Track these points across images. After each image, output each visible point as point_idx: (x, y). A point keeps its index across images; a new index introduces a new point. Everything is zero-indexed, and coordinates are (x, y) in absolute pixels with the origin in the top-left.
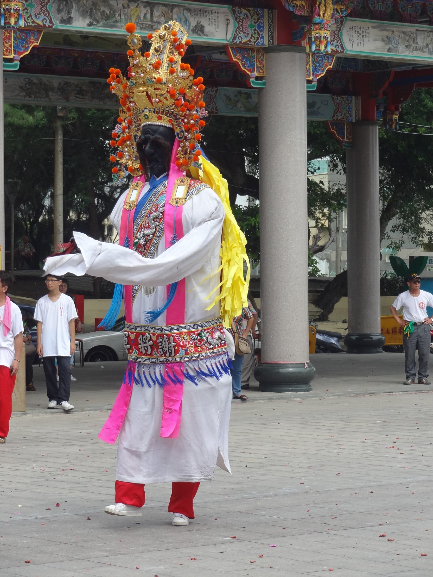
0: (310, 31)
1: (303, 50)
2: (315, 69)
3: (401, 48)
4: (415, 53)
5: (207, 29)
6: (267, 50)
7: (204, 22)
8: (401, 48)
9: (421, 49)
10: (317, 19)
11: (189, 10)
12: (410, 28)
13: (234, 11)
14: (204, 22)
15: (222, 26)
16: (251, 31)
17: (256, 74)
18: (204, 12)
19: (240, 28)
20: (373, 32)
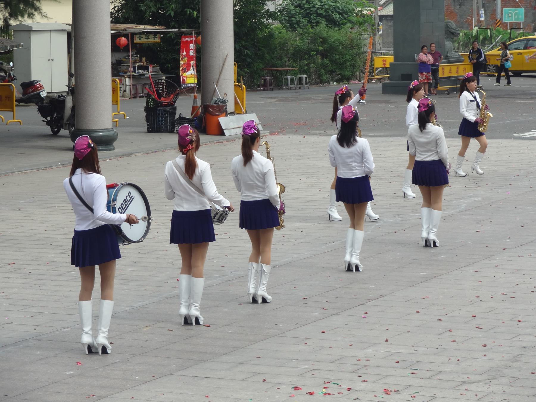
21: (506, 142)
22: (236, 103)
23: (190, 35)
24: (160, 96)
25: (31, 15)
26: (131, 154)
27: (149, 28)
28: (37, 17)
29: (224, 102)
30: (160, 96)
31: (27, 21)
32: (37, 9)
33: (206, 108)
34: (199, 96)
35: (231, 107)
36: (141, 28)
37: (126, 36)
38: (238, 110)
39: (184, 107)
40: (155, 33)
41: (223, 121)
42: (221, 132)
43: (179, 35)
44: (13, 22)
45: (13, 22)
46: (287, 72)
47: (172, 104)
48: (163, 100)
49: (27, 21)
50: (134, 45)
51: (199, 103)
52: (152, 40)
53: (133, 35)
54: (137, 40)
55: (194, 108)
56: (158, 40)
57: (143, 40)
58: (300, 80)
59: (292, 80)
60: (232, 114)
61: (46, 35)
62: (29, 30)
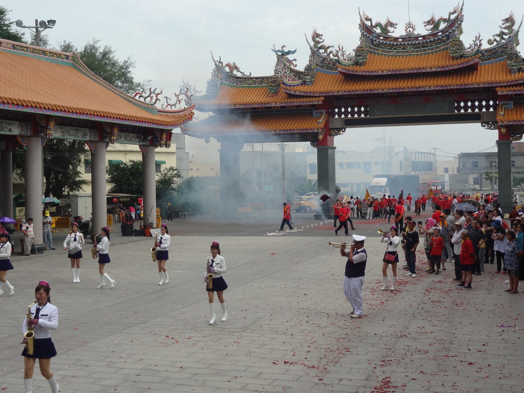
0: (46, 131)
1: (41, 136)
2: (42, 143)
3: (66, 135)
4: (70, 137)
5: (13, 130)
6: (29, 137)
7: (12, 127)
8: (66, 135)
9: (72, 135)
10: (49, 127)
11: (7, 123)
12: (69, 128)
13: (20, 124)
14: (12, 127)
15: (17, 129)
16: (25, 130)
17: (25, 145)
18: (11, 124)
19: (22, 130)
20: (59, 130)
21: (261, 237)
22: (157, 224)
23: (142, 197)
24: (127, 222)
25: (78, 190)
26: (114, 245)
27: (125, 195)
28: (81, 191)
29: (152, 224)
30: (127, 222)
31: (77, 193)
32: (81, 188)
33: (145, 226)
34: (142, 221)
35: (155, 225)
36: (122, 195)
37: (116, 198)
38: (157, 227)
39: (137, 226)
40: (128, 197)
41: (152, 231)
42: (151, 235)
43: (137, 197)
44: (71, 193)
45: (71, 193)
46: (180, 211)
47: (132, 225)
48: (128, 223)
49: (77, 193)
50: (120, 202)
51: (142, 224)
52: (126, 200)
53: (119, 198)
54: (120, 200)
55: (141, 226)
56: (129, 200)
57: (123, 200)
58: (185, 215)
59: (182, 214)
60: (155, 228)
61: (84, 198)
62: (77, 196)
